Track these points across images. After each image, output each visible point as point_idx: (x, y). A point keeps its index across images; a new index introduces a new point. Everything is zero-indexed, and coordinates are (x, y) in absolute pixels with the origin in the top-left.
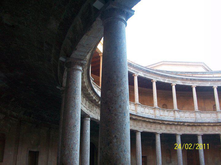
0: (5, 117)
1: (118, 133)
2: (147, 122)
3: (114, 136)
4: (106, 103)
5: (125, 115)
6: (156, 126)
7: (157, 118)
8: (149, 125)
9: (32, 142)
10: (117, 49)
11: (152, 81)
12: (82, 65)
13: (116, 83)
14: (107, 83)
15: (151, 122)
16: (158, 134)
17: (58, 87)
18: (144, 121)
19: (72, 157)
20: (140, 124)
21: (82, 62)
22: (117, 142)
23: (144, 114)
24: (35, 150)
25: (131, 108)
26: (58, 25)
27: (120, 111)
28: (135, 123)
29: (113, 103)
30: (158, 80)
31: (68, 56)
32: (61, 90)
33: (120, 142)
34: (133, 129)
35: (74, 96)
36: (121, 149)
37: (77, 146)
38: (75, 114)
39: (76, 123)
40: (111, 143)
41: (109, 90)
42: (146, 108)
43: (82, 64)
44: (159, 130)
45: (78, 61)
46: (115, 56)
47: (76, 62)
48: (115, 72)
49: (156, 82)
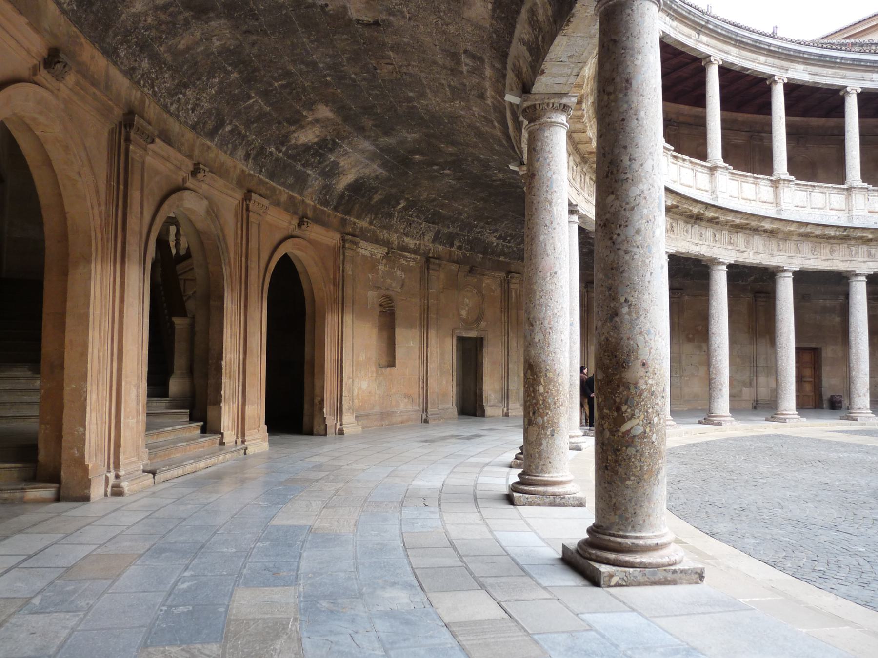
0: (388, 253)
1: (633, 293)
2: (817, 237)
3: (623, 300)
4: (605, 225)
5: (650, 252)
6: (853, 248)
7: (856, 223)
8: (825, 250)
9: (464, 313)
10: (631, 84)
11: (841, 93)
12: (565, 108)
13: (628, 176)
14: (607, 176)
15: (834, 238)
16: (857, 275)
17: (512, 167)
18: (806, 236)
19: (551, 349)
20: (790, 245)
21: (565, 101)
22: (629, 313)
23: (808, 210)
24: (473, 334)
25: (758, 196)
26: (490, 6)
27: (638, 243)
28: (774, 244)
29: (620, 226)
30: (868, 85)
31: (526, 89)
32: (521, 173)
33: (637, 313)
34: (764, 263)
35: (549, 197)
36: (640, 328)
37: (561, 322)
38: (553, 243)
39: (558, 265)
40: (617, 315)
41: (612, 193)
42: (816, 189)
43: (565, 106)
44: (864, 262)
45: (552, 101)
46: (626, 106)
47: (548, 105)
48: (625, 147)
49: (858, 94)
